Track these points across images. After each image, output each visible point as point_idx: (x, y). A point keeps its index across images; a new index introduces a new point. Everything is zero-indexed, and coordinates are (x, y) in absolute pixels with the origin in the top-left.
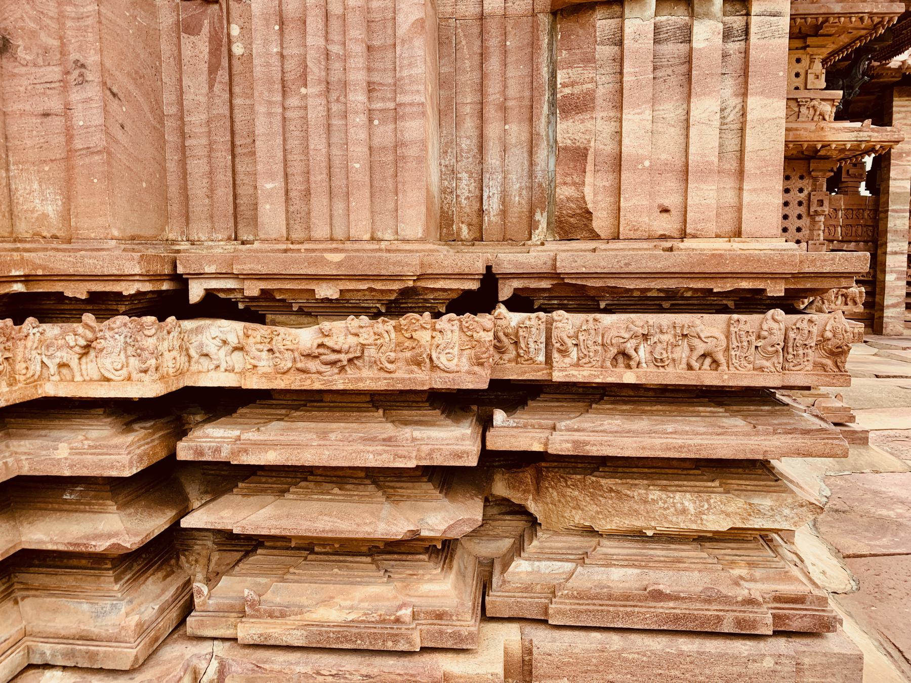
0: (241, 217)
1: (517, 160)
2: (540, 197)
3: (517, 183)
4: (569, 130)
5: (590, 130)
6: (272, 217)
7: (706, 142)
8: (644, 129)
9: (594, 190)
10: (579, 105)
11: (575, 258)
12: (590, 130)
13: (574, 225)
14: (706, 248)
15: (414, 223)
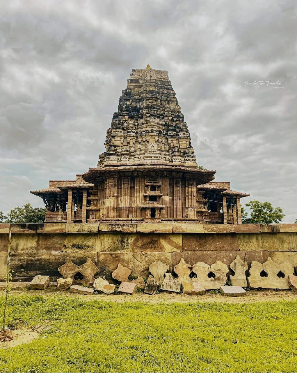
0: (173, 217)
1: (184, 214)
2: (185, 216)
3: (184, 215)
4: (187, 213)
5: (188, 213)
6: (175, 217)
7: (193, 214)
8: (190, 213)
9: (188, 216)
10: (188, 212)
11: (188, 219)
12: (188, 213)
13: (187, 217)
14: (193, 219)
15: (181, 217)
